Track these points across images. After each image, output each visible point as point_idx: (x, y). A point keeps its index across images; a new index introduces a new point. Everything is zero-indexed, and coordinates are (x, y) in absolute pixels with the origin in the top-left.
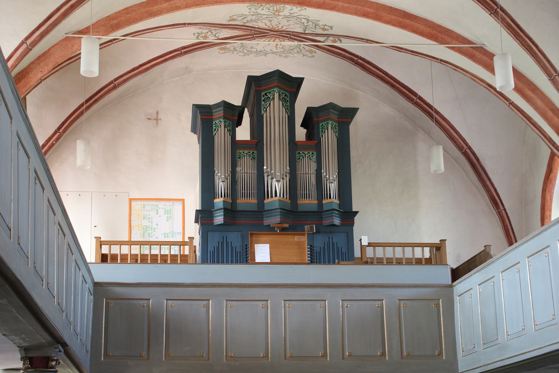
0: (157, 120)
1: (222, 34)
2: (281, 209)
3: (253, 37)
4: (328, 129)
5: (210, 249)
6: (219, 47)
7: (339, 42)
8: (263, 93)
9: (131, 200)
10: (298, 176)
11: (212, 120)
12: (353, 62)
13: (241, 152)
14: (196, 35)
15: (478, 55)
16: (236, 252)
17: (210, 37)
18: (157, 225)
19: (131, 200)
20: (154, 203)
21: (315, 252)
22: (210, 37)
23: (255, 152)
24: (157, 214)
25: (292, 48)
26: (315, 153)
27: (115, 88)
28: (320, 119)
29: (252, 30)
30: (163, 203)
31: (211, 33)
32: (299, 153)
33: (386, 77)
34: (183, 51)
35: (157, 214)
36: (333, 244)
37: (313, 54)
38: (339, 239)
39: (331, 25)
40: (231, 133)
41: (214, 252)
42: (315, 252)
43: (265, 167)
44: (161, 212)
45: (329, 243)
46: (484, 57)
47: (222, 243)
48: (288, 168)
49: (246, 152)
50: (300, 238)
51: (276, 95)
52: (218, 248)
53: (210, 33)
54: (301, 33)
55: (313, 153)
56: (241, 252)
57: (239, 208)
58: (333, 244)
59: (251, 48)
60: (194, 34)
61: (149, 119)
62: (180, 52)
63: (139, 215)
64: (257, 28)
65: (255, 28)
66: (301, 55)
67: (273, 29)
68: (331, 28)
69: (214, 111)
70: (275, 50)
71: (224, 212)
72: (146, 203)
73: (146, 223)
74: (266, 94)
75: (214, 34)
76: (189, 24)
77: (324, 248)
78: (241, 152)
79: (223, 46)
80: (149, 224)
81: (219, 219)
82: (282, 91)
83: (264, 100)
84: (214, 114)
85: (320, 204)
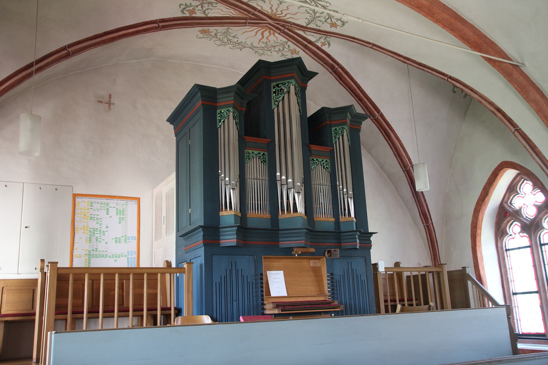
0: (109, 104)
2: (307, 229)
4: (343, 136)
6: (200, 29)
7: (327, 46)
8: (273, 84)
9: (75, 196)
10: (313, 186)
11: (215, 109)
13: (250, 152)
14: (182, 7)
15: (516, 75)
16: (248, 283)
18: (107, 227)
19: (75, 196)
20: (104, 201)
22: (198, 12)
23: (266, 153)
24: (108, 214)
26: (328, 161)
27: (68, 56)
28: (333, 123)
29: (249, 12)
30: (115, 201)
31: (202, 7)
32: (313, 159)
33: (358, 90)
34: (160, 24)
35: (108, 214)
36: (352, 270)
38: (358, 265)
41: (220, 284)
43: (278, 174)
44: (113, 212)
45: (348, 270)
46: (521, 77)
49: (256, 152)
50: (315, 263)
53: (200, 8)
55: (326, 161)
56: (254, 282)
57: (250, 225)
58: (352, 270)
59: (234, 37)
61: (101, 102)
62: (157, 25)
63: (85, 215)
64: (259, 11)
67: (273, 17)
68: (343, 23)
69: (219, 97)
71: (237, 231)
72: (93, 200)
73: (93, 224)
74: (278, 85)
75: (204, 9)
77: (344, 276)
78: (250, 152)
79: (206, 28)
80: (98, 226)
81: (229, 239)
83: (275, 92)
84: (218, 101)
85: (337, 222)
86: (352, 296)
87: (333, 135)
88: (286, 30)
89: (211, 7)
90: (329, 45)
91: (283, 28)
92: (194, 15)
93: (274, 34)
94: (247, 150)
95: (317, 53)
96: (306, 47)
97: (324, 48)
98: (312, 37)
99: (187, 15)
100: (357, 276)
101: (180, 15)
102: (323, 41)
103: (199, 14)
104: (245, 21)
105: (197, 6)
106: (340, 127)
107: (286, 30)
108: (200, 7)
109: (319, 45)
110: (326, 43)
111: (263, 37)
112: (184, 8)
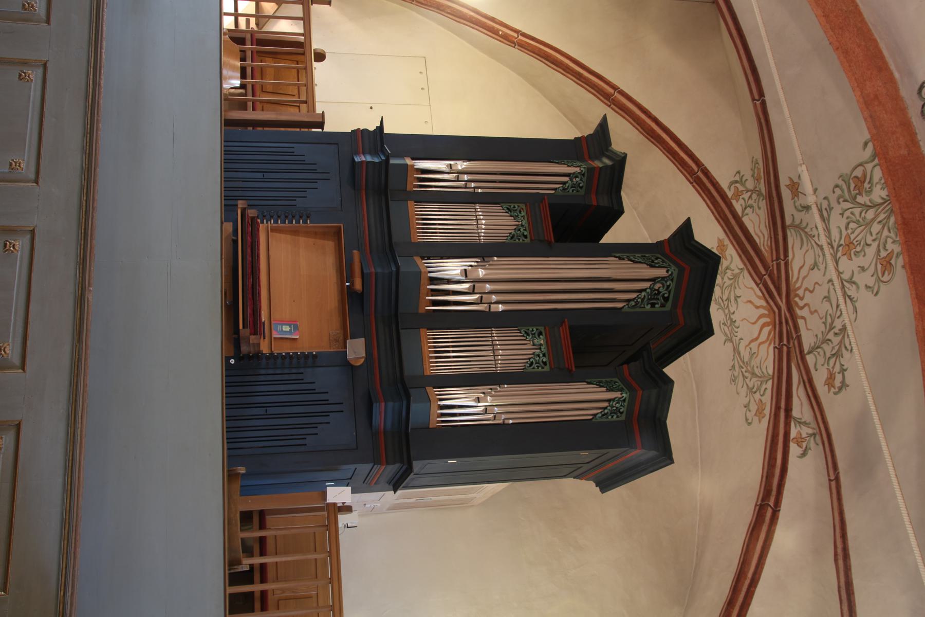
1: (753, 216)
3: (761, 277)
5: (298, 149)
6: (722, 235)
7: (800, 451)
12: (763, 500)
13: (523, 214)
14: (737, 178)
17: (741, 201)
21: (301, 370)
22: (741, 201)
25: (757, 371)
31: (750, 197)
32: (540, 334)
33: (747, 582)
34: (700, 174)
36: (326, 414)
37: (756, 419)
39: (847, 381)
40: (560, 193)
41: (292, 154)
42: (301, 370)
45: (326, 402)
47: (314, 171)
48: (501, 308)
51: (662, 272)
52: (302, 162)
53: (746, 196)
54: (801, 351)
55: (545, 363)
59: (736, 297)
60: (738, 172)
65: (786, 255)
66: (746, 401)
67: (792, 295)
70: (742, 348)
75: (750, 202)
76: (764, 104)
77: (312, 392)
82: (673, 287)
86: (271, 411)
87: (604, 380)
88: (785, 348)
89: (755, 205)
90: (804, 454)
91: (785, 342)
92: (734, 202)
93: (770, 344)
94: (524, 207)
95: (777, 444)
96: (778, 408)
97: (793, 447)
98: (800, 407)
99: (730, 194)
100: (304, 190)
101: (724, 185)
102: (804, 435)
103: (738, 206)
104: (763, 272)
105: (748, 191)
106: (622, 386)
107: (785, 348)
108: (749, 194)
109: (793, 433)
110: (804, 444)
111: (757, 339)
112: (736, 182)
